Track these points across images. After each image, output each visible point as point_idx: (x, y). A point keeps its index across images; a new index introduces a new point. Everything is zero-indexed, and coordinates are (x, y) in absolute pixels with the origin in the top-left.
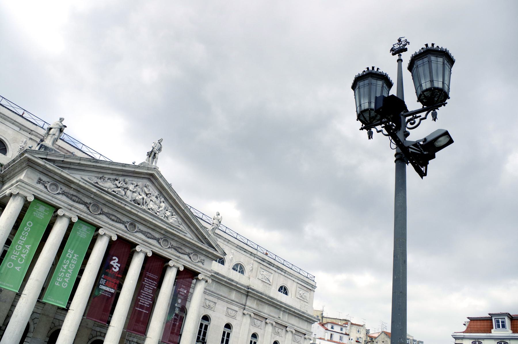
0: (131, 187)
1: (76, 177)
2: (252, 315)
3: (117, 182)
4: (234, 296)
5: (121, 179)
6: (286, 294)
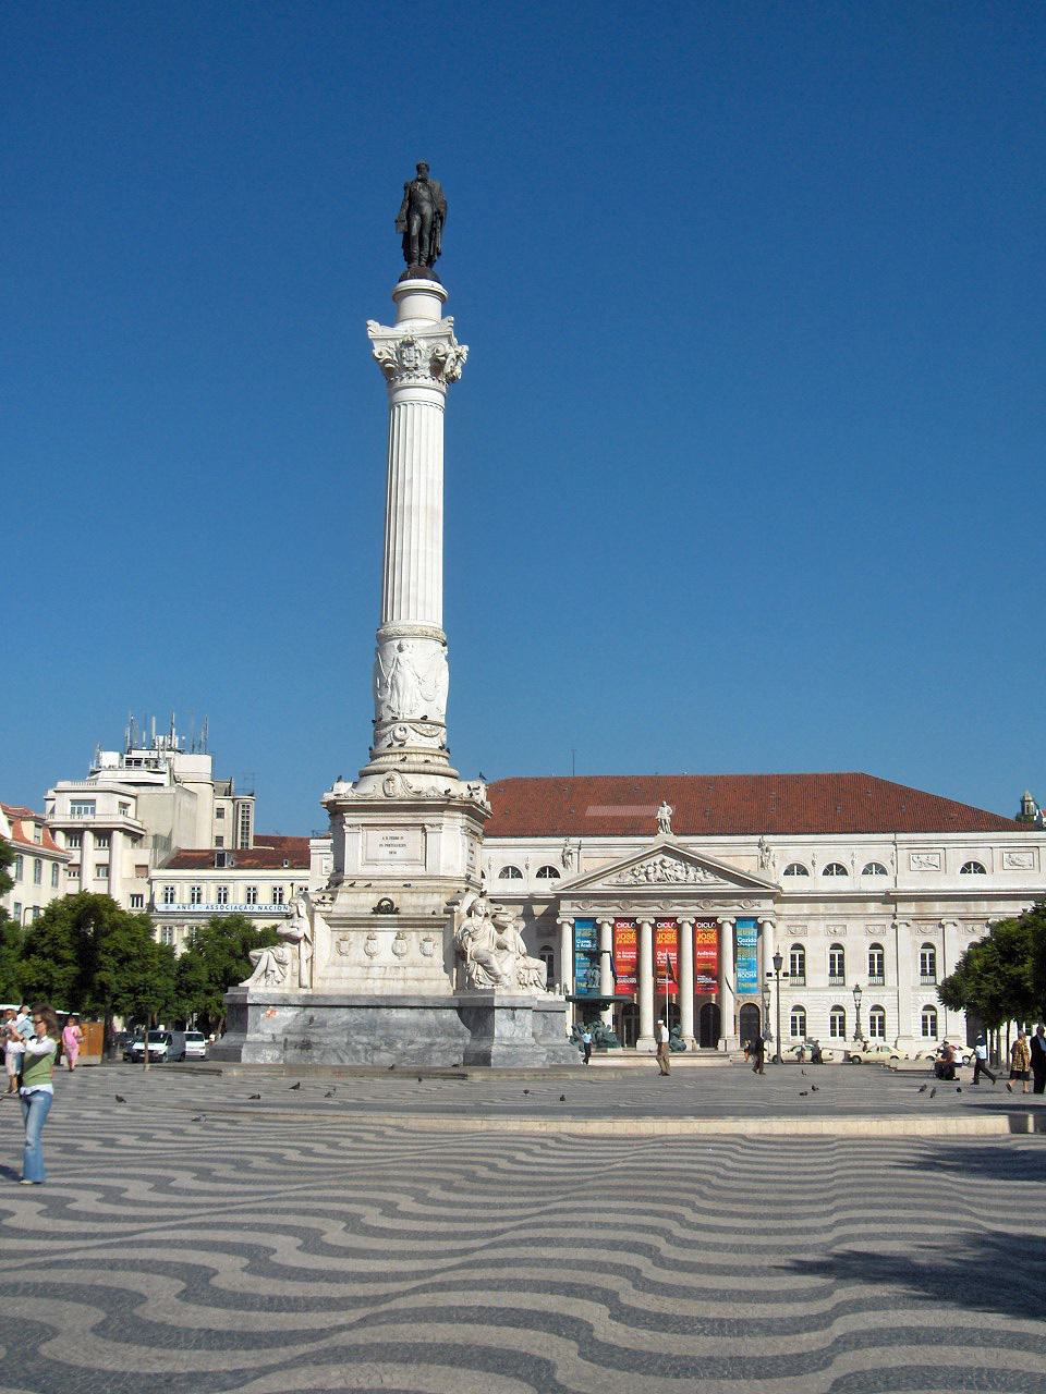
0: (651, 870)
1: (598, 886)
2: (911, 923)
3: (635, 872)
4: (873, 907)
5: (637, 866)
6: (982, 871)
